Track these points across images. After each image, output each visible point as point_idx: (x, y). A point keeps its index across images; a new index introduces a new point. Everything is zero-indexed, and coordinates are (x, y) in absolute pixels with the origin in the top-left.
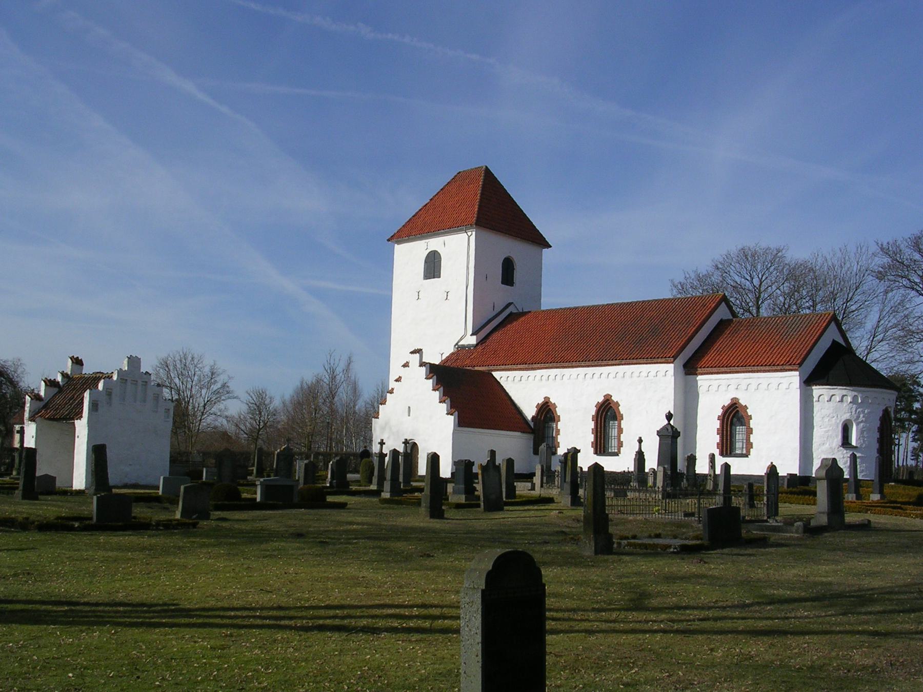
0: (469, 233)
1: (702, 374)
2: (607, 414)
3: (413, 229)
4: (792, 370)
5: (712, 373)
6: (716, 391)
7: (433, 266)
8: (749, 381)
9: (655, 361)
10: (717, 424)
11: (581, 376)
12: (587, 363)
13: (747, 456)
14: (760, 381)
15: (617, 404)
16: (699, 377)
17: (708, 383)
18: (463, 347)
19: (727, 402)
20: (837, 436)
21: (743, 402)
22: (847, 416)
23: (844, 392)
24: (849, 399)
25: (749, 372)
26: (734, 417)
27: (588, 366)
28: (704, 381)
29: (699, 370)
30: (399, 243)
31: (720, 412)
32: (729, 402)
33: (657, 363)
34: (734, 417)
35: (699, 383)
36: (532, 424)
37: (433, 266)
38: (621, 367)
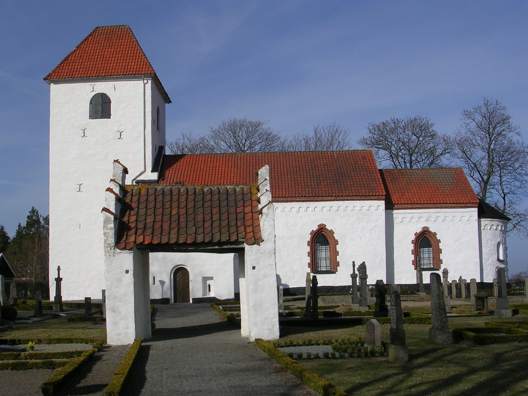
0: (146, 81)
1: (398, 209)
2: (321, 238)
3: (69, 70)
4: (472, 207)
6: (410, 222)
7: (101, 107)
8: (438, 215)
9: (368, 198)
10: (412, 247)
11: (295, 210)
12: (303, 199)
14: (447, 214)
16: (395, 211)
17: (402, 216)
18: (144, 182)
19: (419, 230)
20: (495, 254)
21: (432, 230)
22: (499, 240)
23: (498, 223)
24: (500, 228)
25: (438, 208)
26: (425, 240)
27: (303, 201)
28: (398, 214)
29: (396, 206)
30: (56, 82)
31: (413, 238)
32: (421, 230)
33: (370, 200)
34: (425, 240)
35: (395, 216)
37: (101, 107)
38: (336, 202)
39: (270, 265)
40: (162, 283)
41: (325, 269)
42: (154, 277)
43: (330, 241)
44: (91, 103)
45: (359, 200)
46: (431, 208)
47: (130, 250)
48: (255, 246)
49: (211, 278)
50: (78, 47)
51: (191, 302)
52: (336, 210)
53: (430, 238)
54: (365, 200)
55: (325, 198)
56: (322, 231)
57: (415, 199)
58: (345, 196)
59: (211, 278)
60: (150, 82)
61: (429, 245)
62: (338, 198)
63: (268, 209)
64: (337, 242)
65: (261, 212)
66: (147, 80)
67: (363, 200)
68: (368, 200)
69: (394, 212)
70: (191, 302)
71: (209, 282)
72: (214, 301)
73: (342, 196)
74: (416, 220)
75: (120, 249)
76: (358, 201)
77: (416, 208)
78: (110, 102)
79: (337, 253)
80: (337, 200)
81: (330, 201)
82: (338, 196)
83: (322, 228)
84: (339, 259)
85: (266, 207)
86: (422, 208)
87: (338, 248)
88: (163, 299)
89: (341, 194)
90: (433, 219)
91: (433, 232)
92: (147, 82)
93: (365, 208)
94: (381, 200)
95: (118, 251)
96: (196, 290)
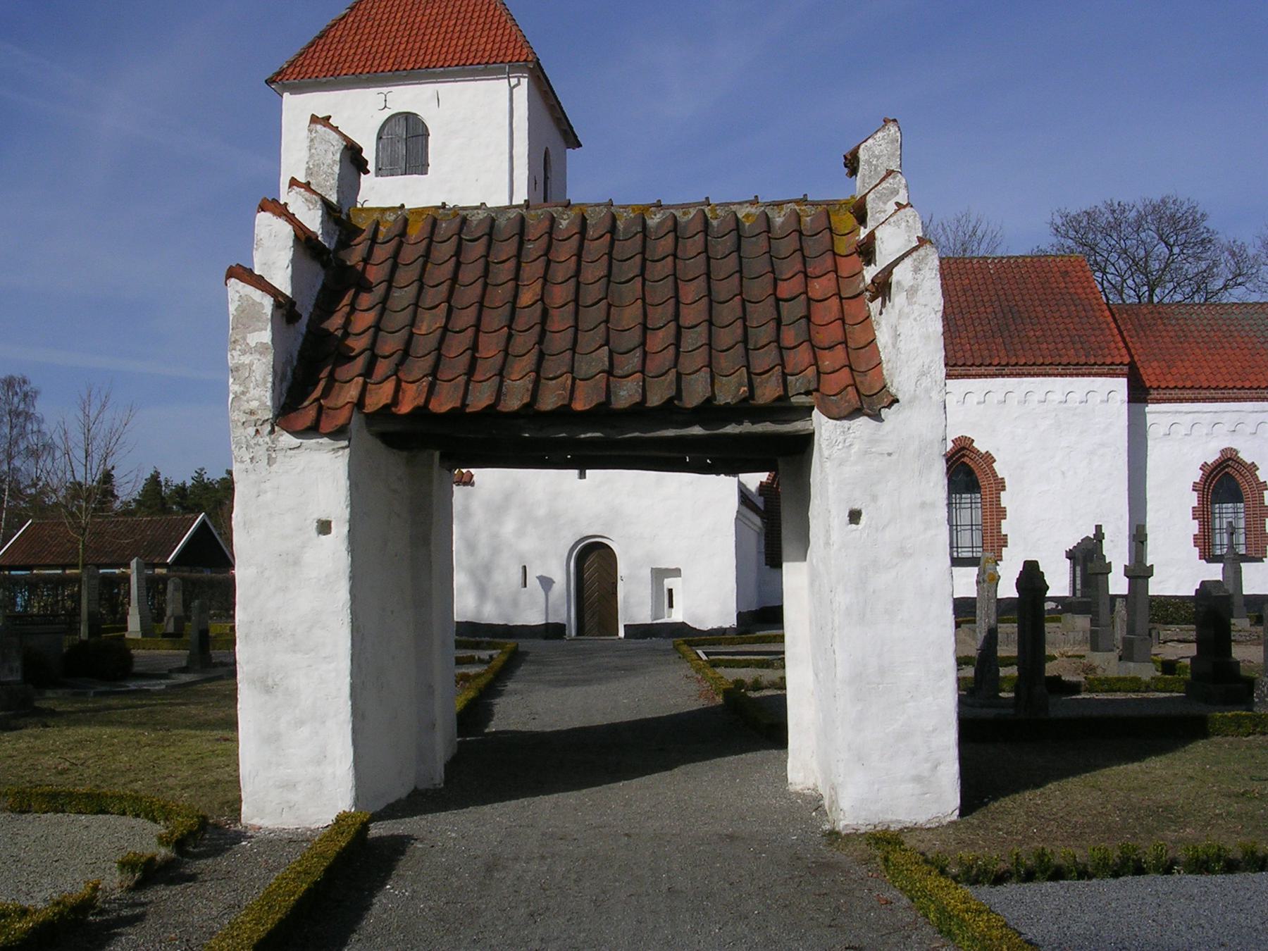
0: (514, 81)
1: (1158, 401)
5: (1181, 400)
8: (1261, 417)
9: (1084, 370)
10: (1193, 499)
13: (1260, 560)
15: (989, 459)
16: (1151, 408)
17: (1170, 419)
19: (1212, 457)
21: (1246, 457)
28: (1158, 415)
31: (1197, 476)
32: (1217, 456)
33: (1089, 375)
35: (1150, 419)
36: (760, 502)
38: (999, 380)
39: (923, 505)
40: (546, 583)
41: (970, 555)
42: (525, 567)
43: (983, 482)
44: (379, 138)
45: (1062, 376)
46: (1245, 400)
47: (337, 434)
48: (862, 422)
49: (676, 572)
50: (352, 9)
51: (622, 634)
52: (999, 402)
53: (1237, 477)
54: (1077, 375)
55: (973, 370)
56: (964, 456)
57: (1202, 377)
58: (1025, 364)
59: (676, 572)
60: (524, 82)
61: (1235, 495)
62: (1007, 371)
63: (917, 270)
64: (1000, 485)
65: (882, 287)
66: (519, 78)
67: (1071, 375)
68: (1083, 375)
69: (1147, 409)
70: (622, 634)
71: (669, 583)
72: (681, 631)
73: (1016, 364)
74: (1205, 431)
75: (296, 434)
76: (1059, 379)
77: (1204, 400)
78: (426, 134)
79: (1002, 513)
80: (1003, 376)
81: (986, 376)
82: (1007, 365)
83: (963, 448)
84: (1005, 527)
85: (908, 262)
86: (1222, 400)
87: (1006, 499)
88: (547, 625)
89: (1013, 361)
90: (1250, 429)
91: (1249, 462)
92: (519, 84)
93: (1076, 397)
94: (1118, 375)
95: (287, 439)
96: (635, 605)
